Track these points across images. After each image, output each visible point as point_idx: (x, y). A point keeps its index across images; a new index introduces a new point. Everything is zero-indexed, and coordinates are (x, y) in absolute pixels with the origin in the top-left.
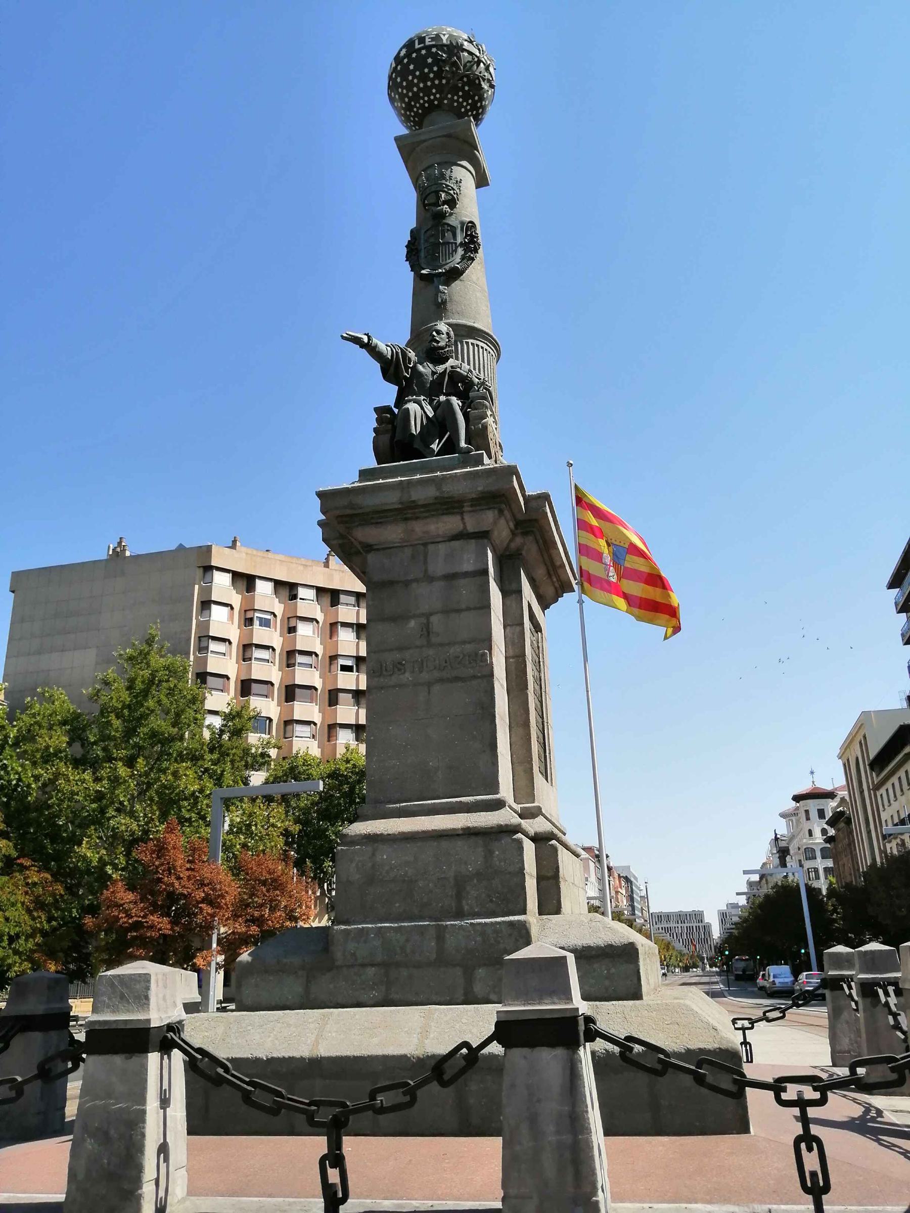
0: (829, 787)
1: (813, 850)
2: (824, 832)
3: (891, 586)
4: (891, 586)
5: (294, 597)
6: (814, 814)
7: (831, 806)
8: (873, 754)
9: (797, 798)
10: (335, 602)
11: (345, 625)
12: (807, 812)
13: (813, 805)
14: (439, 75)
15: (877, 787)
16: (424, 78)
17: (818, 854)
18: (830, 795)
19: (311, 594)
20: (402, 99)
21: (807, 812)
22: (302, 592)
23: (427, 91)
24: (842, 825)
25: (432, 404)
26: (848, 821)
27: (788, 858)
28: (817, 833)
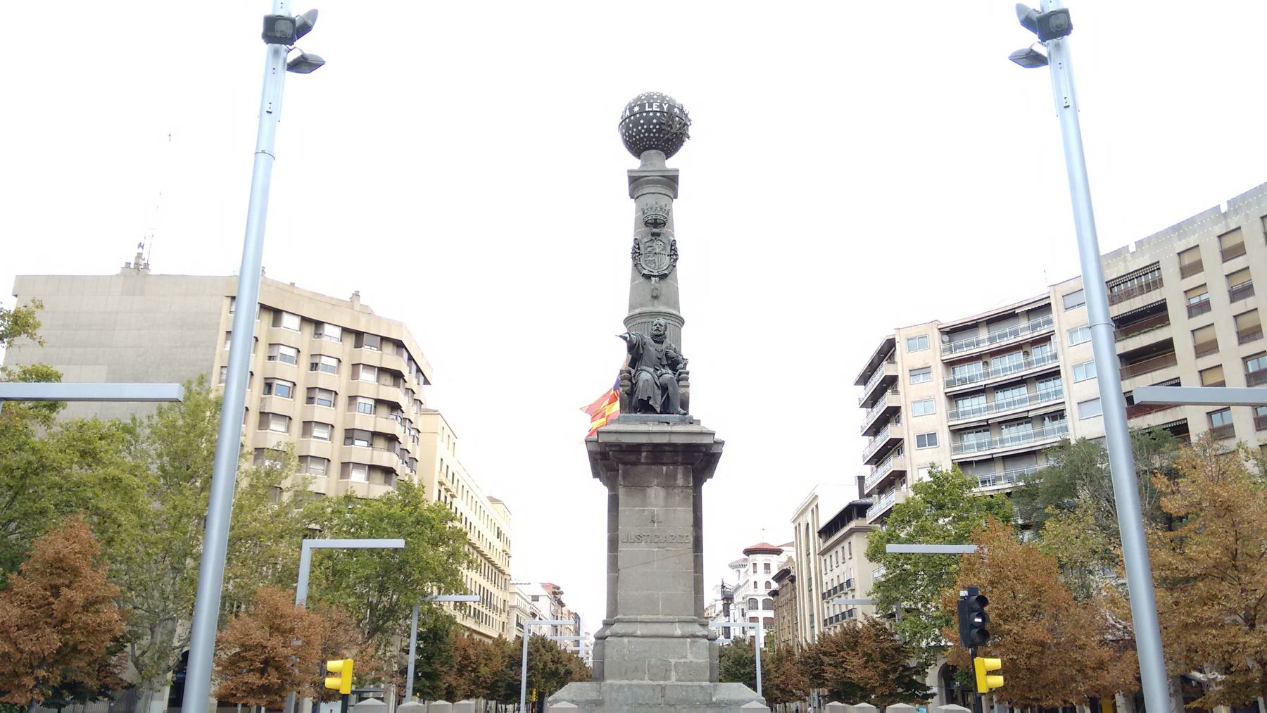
0: (775, 544)
1: (756, 601)
2: (768, 584)
3: (857, 383)
4: (857, 383)
5: (318, 334)
6: (760, 568)
7: (776, 563)
8: (823, 522)
9: (748, 552)
10: (358, 345)
11: (366, 366)
12: (755, 565)
13: (761, 559)
14: (659, 131)
15: (823, 553)
16: (649, 130)
17: (760, 605)
18: (777, 552)
19: (337, 332)
20: (630, 136)
21: (755, 565)
22: (328, 329)
23: (649, 138)
24: (787, 581)
25: (653, 368)
26: (793, 580)
27: (732, 606)
28: (761, 586)
